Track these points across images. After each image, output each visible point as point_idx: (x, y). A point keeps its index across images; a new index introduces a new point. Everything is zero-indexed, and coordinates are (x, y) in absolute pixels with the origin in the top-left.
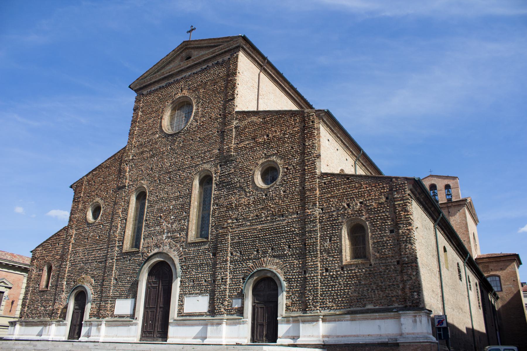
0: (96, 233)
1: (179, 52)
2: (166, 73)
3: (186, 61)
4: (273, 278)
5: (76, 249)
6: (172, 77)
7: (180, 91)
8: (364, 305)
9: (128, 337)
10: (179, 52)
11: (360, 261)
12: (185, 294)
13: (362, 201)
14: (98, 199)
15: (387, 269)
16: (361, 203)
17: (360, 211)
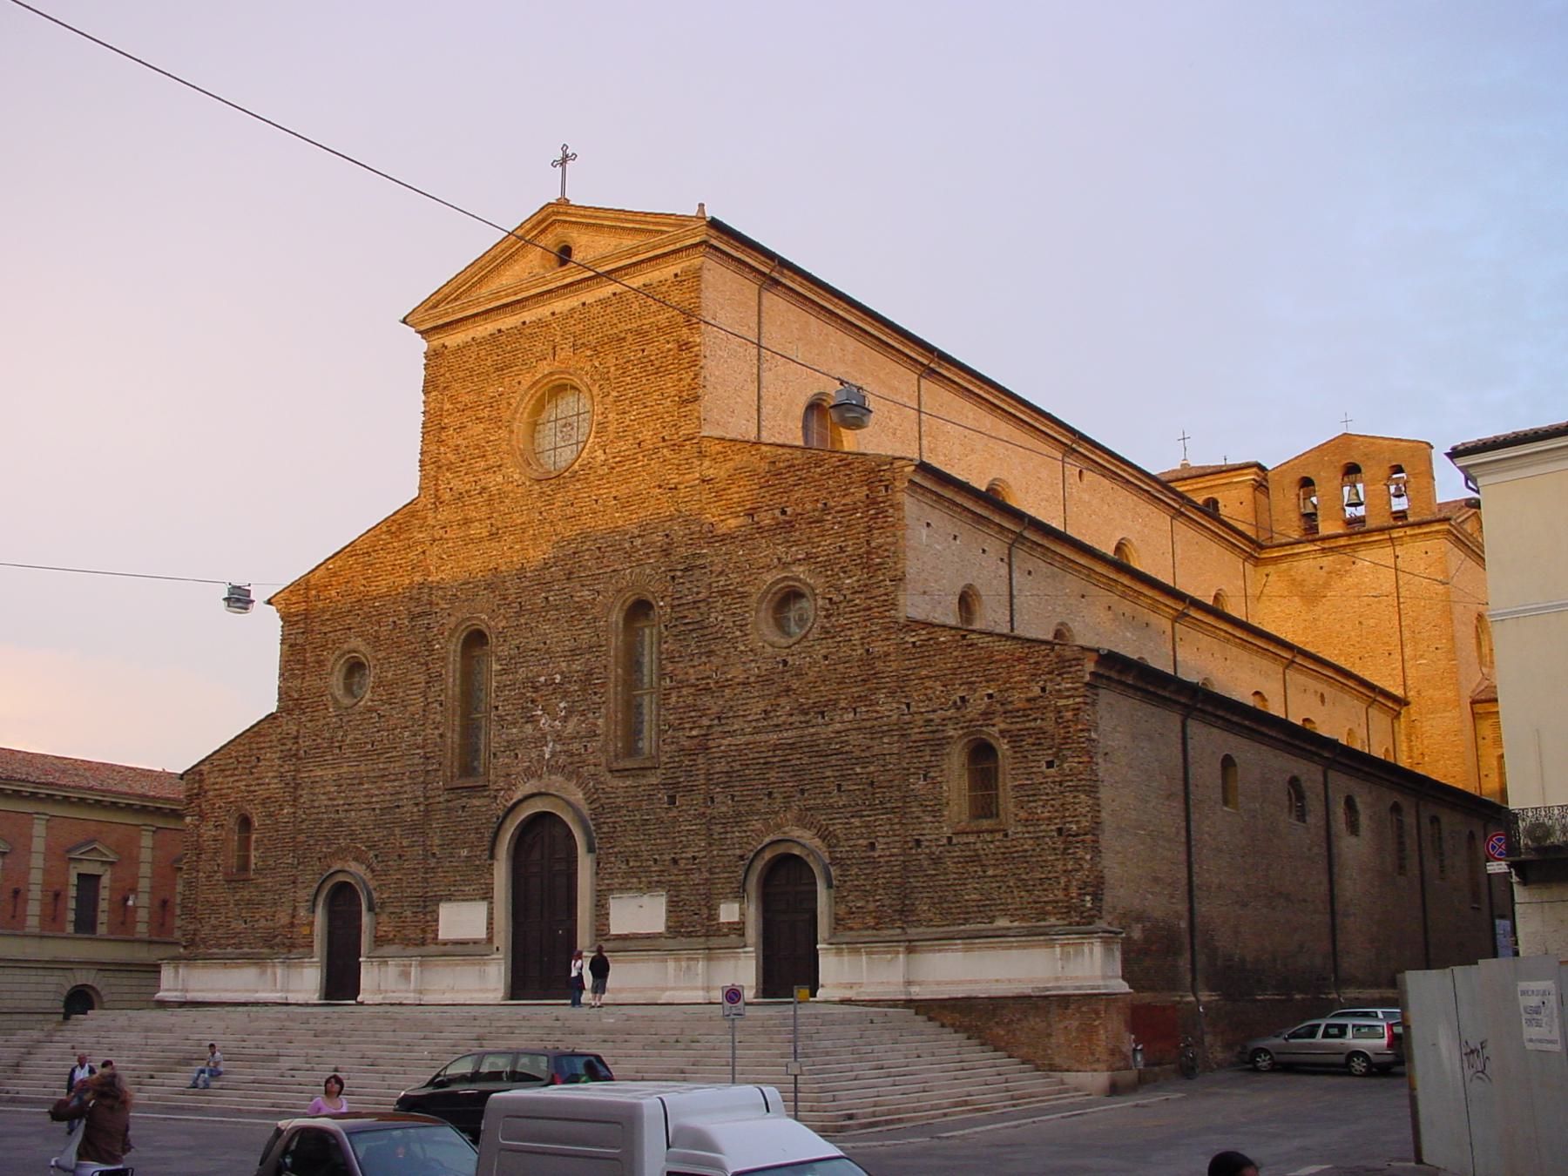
0: (363, 734)
2: (507, 296)
3: (560, 270)
4: (805, 858)
5: (312, 774)
6: (524, 307)
7: (551, 352)
8: (992, 920)
9: (481, 990)
11: (986, 824)
12: (611, 890)
13: (990, 691)
14: (356, 642)
15: (1038, 845)
16: (990, 696)
17: (987, 715)
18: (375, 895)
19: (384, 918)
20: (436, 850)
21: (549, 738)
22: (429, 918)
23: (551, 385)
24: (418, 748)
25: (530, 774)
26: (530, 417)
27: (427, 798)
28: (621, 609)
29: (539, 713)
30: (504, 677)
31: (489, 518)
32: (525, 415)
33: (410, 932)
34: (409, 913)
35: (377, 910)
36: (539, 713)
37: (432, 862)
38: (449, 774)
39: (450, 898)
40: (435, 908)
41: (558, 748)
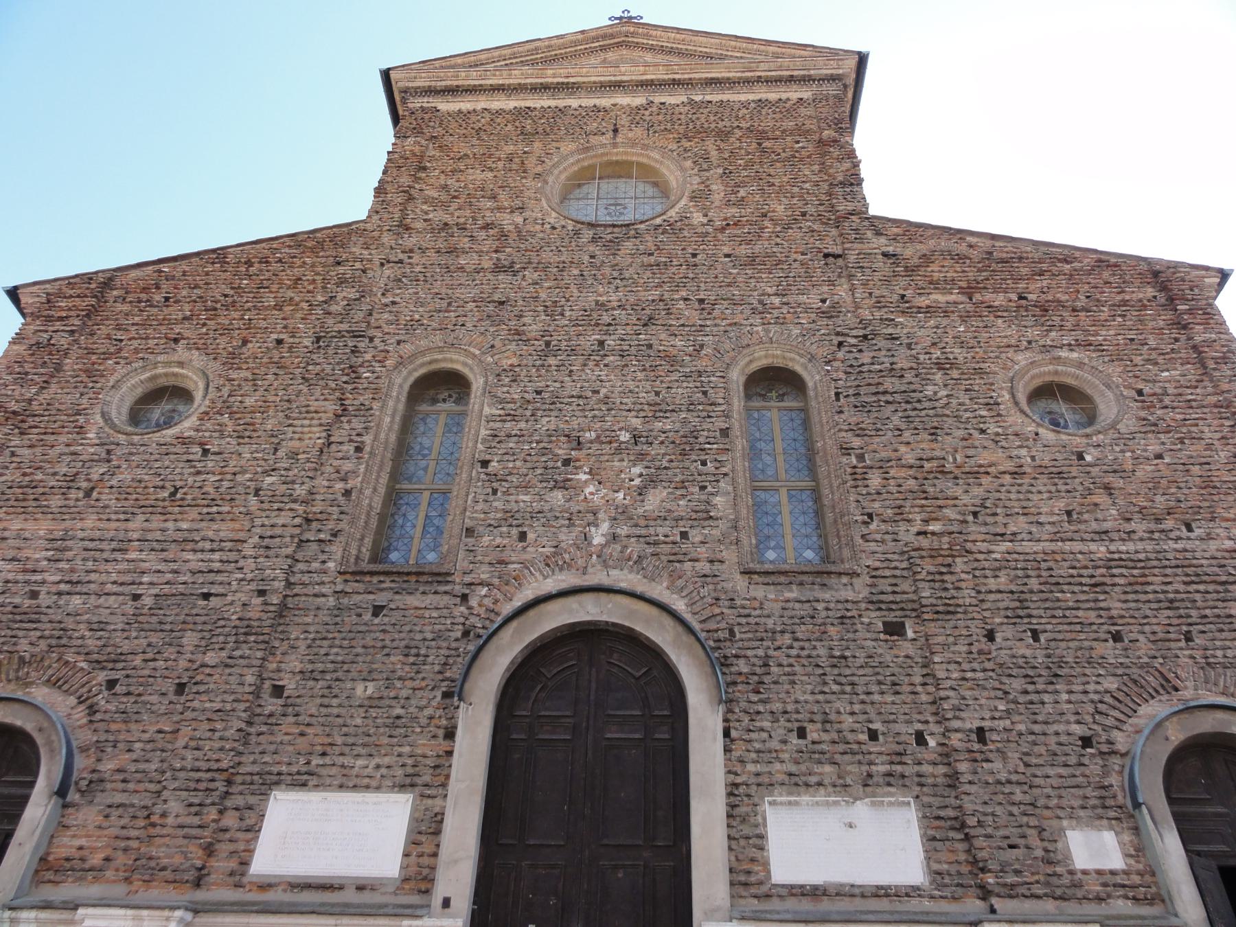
1: (597, 44)
10: (597, 44)
18: (80, 762)
19: (88, 816)
20: (290, 683)
21: (601, 515)
22: (230, 820)
23: (605, 159)
24: (295, 501)
25: (553, 562)
26: (568, 179)
27: (289, 584)
28: (743, 370)
29: (584, 477)
30: (508, 425)
31: (496, 251)
32: (563, 177)
33: (165, 852)
34: (174, 806)
35: (73, 796)
36: (584, 477)
37: (272, 705)
38: (354, 552)
39: (300, 782)
40: (252, 800)
41: (623, 530)
